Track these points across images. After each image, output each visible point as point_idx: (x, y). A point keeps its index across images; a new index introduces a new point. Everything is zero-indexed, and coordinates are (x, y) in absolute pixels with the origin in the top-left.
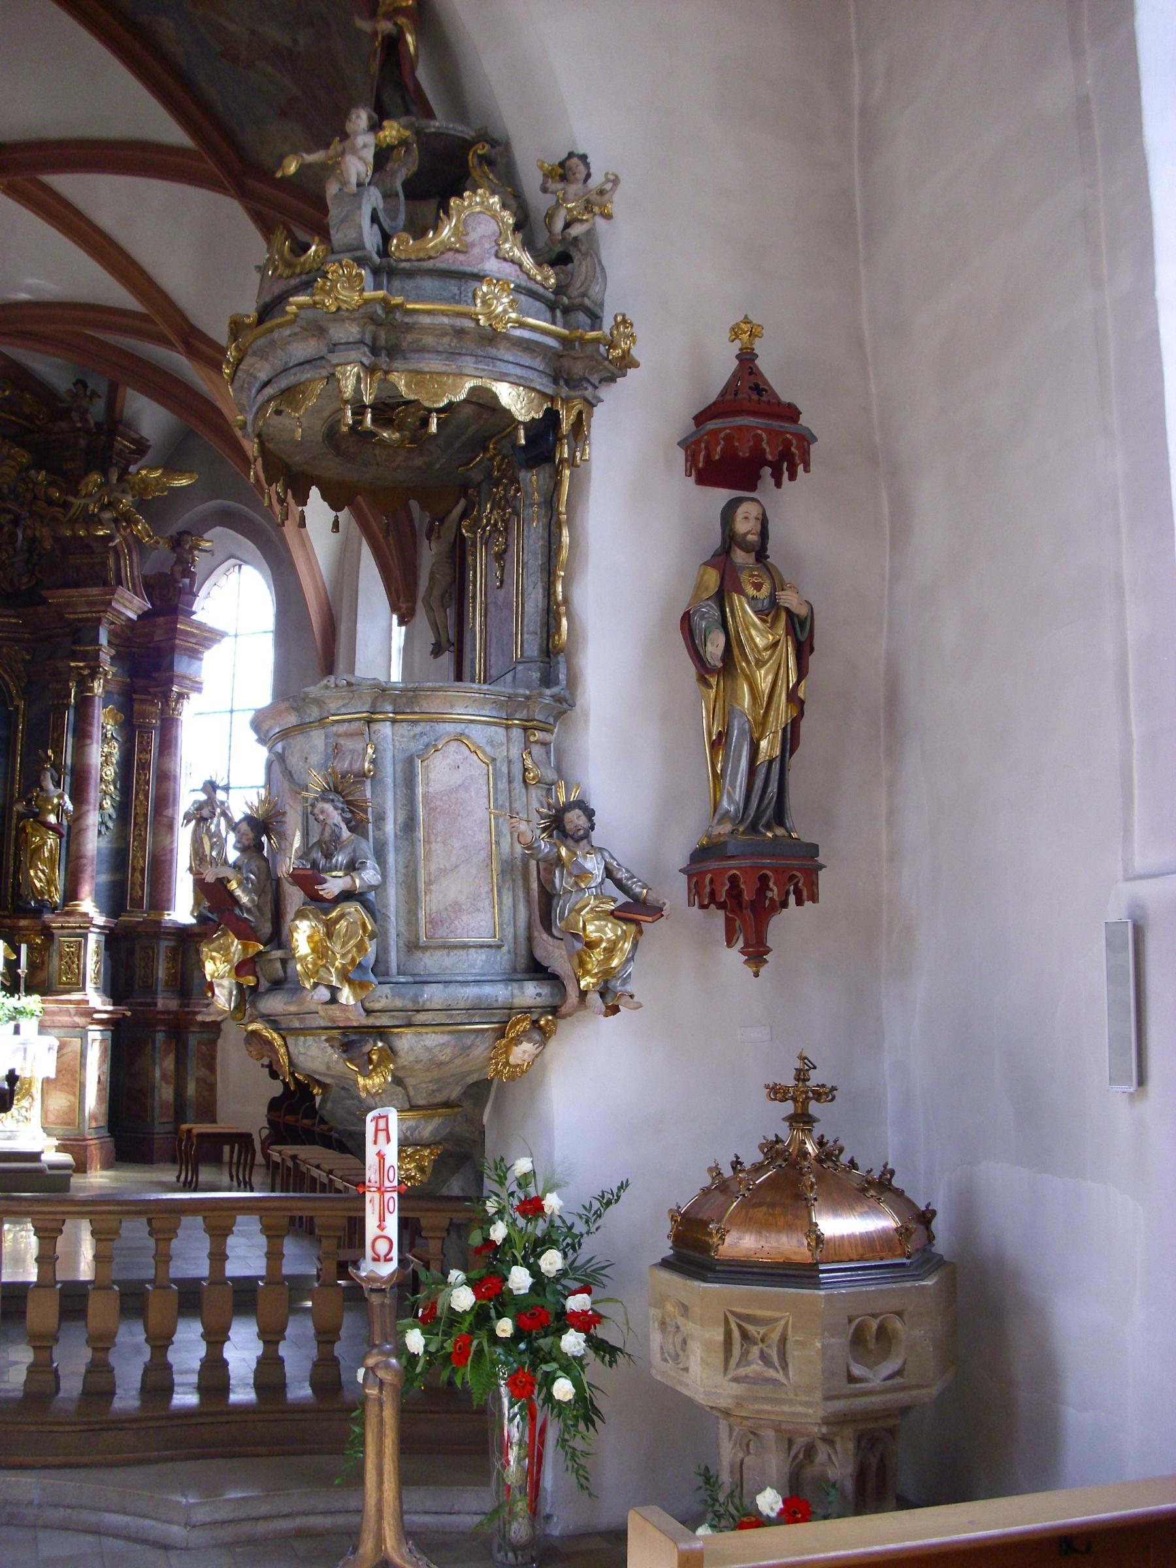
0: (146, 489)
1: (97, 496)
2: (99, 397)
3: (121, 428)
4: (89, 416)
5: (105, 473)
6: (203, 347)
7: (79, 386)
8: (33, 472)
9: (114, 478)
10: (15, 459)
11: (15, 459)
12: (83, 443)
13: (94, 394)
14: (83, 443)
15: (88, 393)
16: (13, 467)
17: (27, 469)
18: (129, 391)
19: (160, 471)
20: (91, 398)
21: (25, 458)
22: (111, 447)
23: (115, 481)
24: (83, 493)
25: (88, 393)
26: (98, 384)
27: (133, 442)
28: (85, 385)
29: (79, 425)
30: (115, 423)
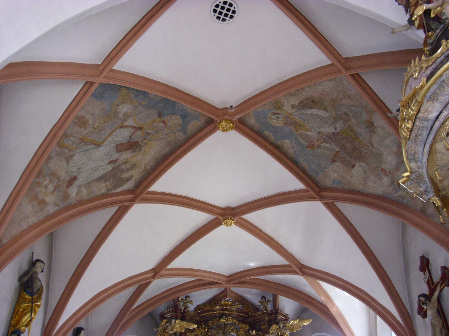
0: (293, 328)
1: (276, 333)
2: (270, 301)
3: (279, 311)
4: (268, 308)
5: (278, 324)
6: (308, 271)
7: (263, 299)
8: (250, 331)
9: (282, 326)
10: (244, 328)
11: (244, 328)
12: (266, 318)
13: (268, 301)
14: (266, 318)
15: (266, 300)
16: (243, 331)
17: (248, 331)
18: (280, 296)
19: (298, 320)
20: (267, 302)
21: (246, 327)
22: (277, 318)
23: (282, 327)
24: (271, 333)
25: (266, 300)
26: (269, 297)
27: (284, 316)
28: (265, 299)
29: (265, 311)
30: (276, 311)
